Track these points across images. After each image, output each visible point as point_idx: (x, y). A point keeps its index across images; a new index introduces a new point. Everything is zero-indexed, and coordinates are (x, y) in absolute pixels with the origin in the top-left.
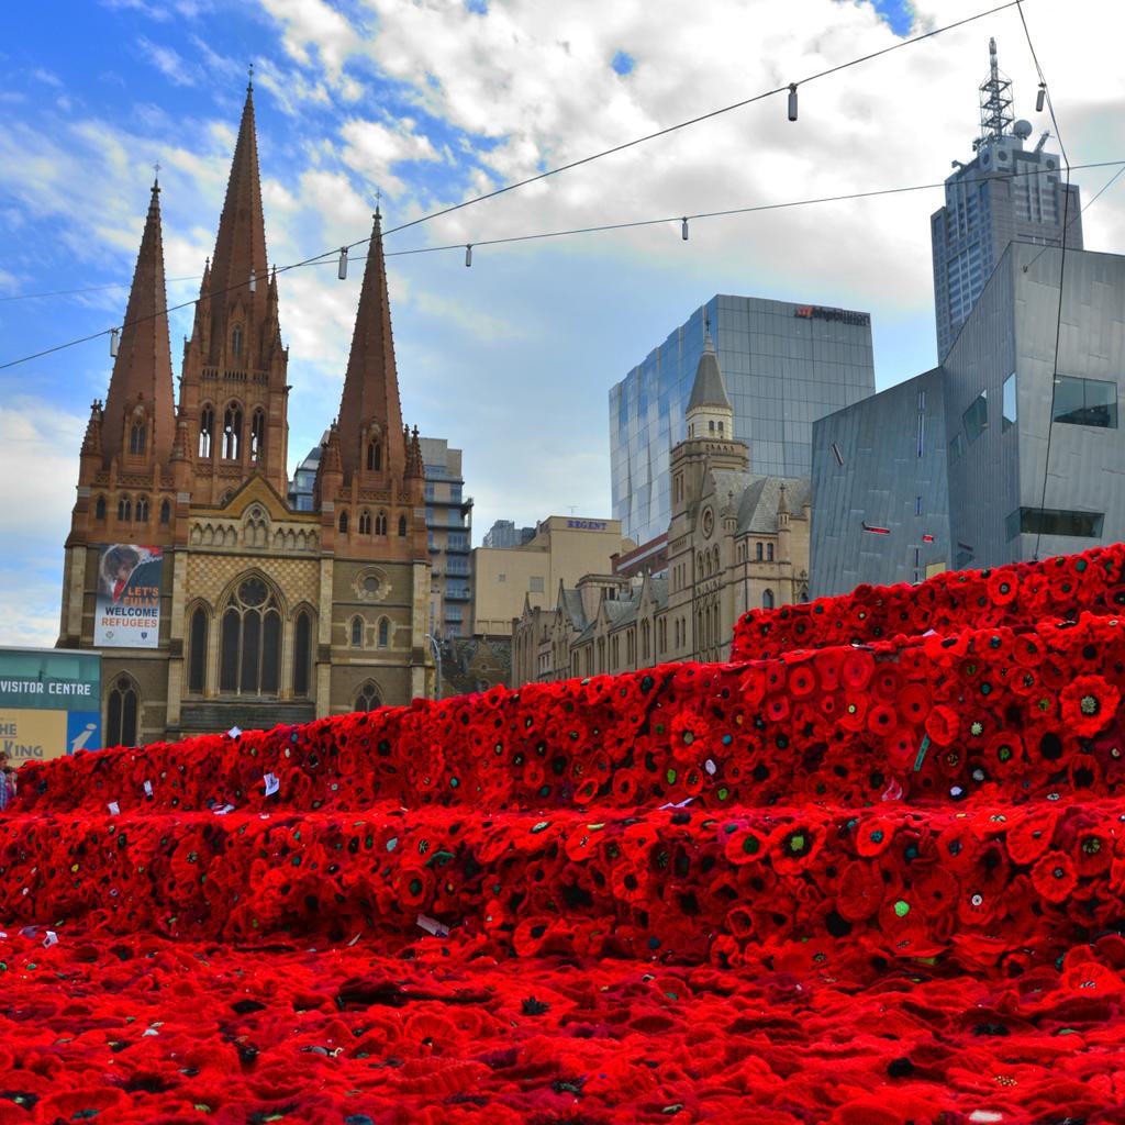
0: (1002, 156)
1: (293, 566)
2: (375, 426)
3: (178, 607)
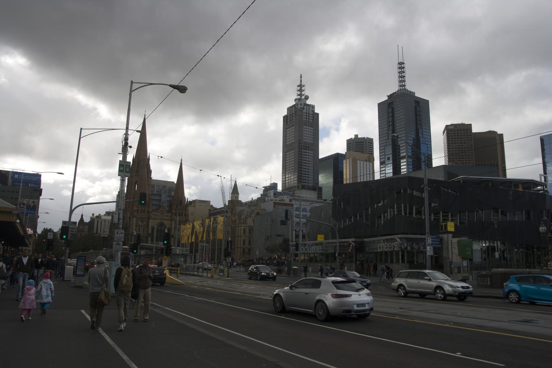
0: (301, 104)
3: (150, 228)
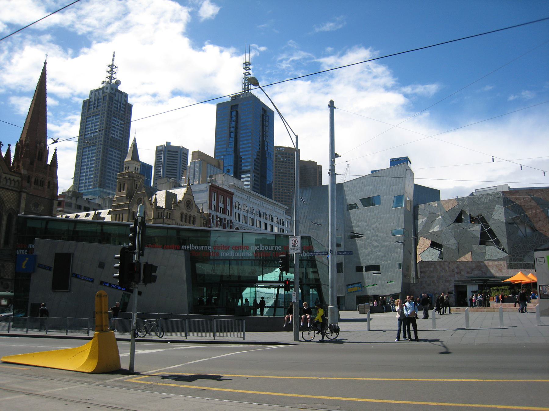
1: (9, 193)
2: (42, 144)
